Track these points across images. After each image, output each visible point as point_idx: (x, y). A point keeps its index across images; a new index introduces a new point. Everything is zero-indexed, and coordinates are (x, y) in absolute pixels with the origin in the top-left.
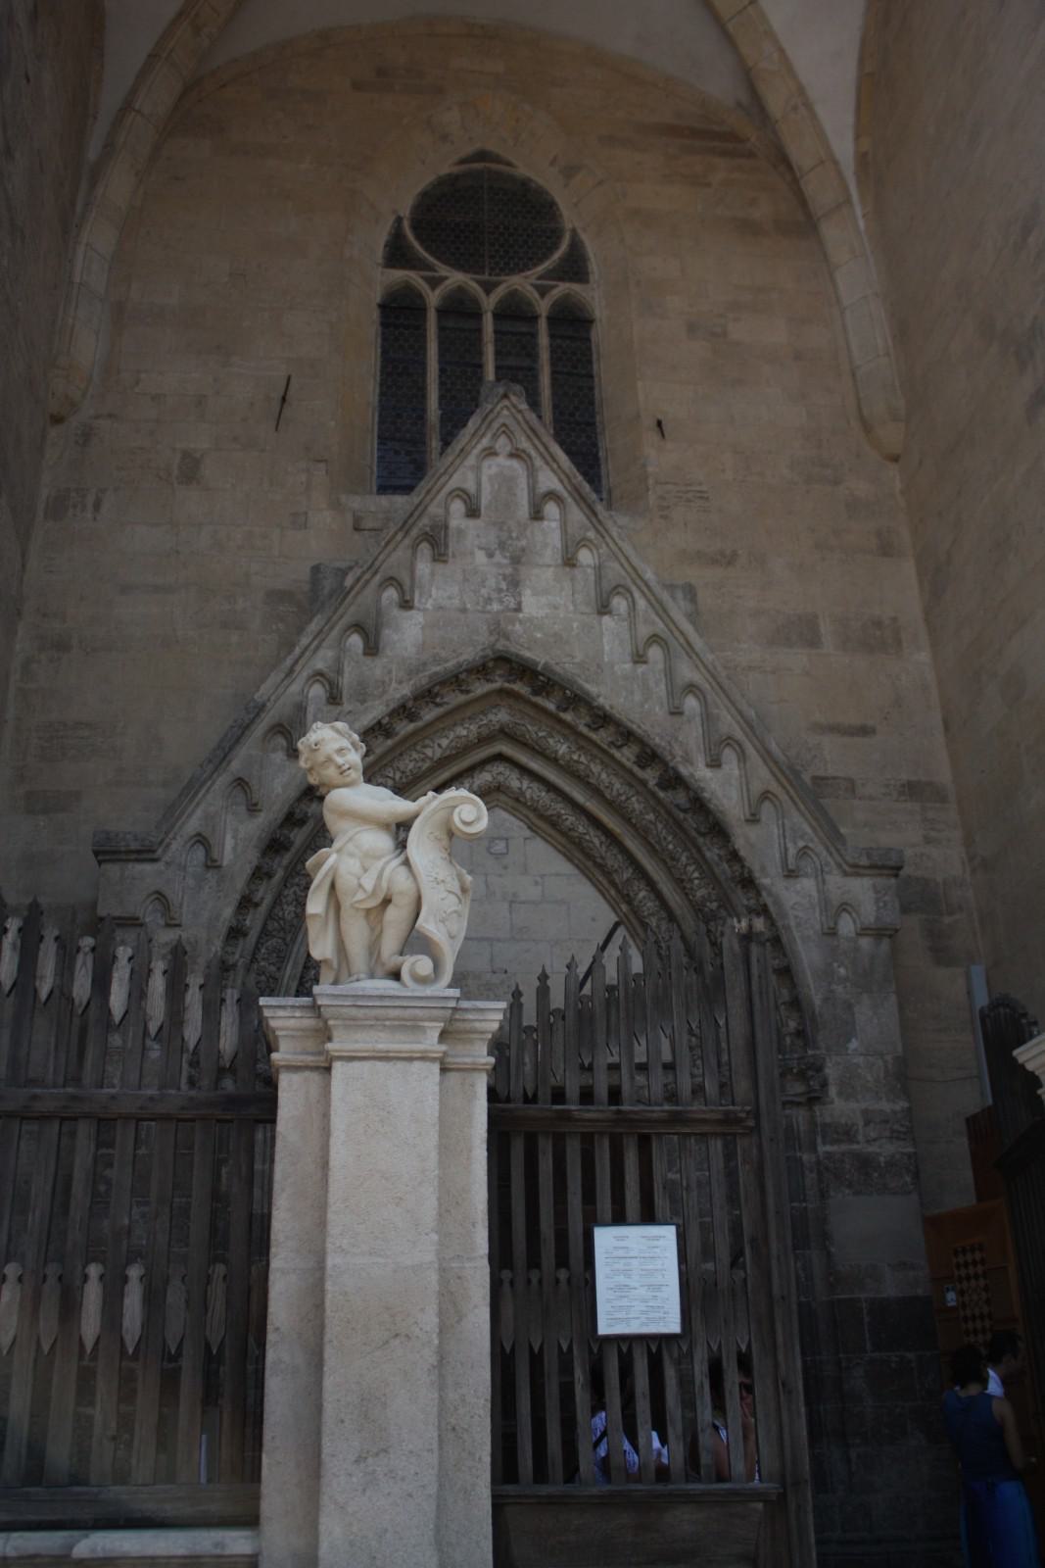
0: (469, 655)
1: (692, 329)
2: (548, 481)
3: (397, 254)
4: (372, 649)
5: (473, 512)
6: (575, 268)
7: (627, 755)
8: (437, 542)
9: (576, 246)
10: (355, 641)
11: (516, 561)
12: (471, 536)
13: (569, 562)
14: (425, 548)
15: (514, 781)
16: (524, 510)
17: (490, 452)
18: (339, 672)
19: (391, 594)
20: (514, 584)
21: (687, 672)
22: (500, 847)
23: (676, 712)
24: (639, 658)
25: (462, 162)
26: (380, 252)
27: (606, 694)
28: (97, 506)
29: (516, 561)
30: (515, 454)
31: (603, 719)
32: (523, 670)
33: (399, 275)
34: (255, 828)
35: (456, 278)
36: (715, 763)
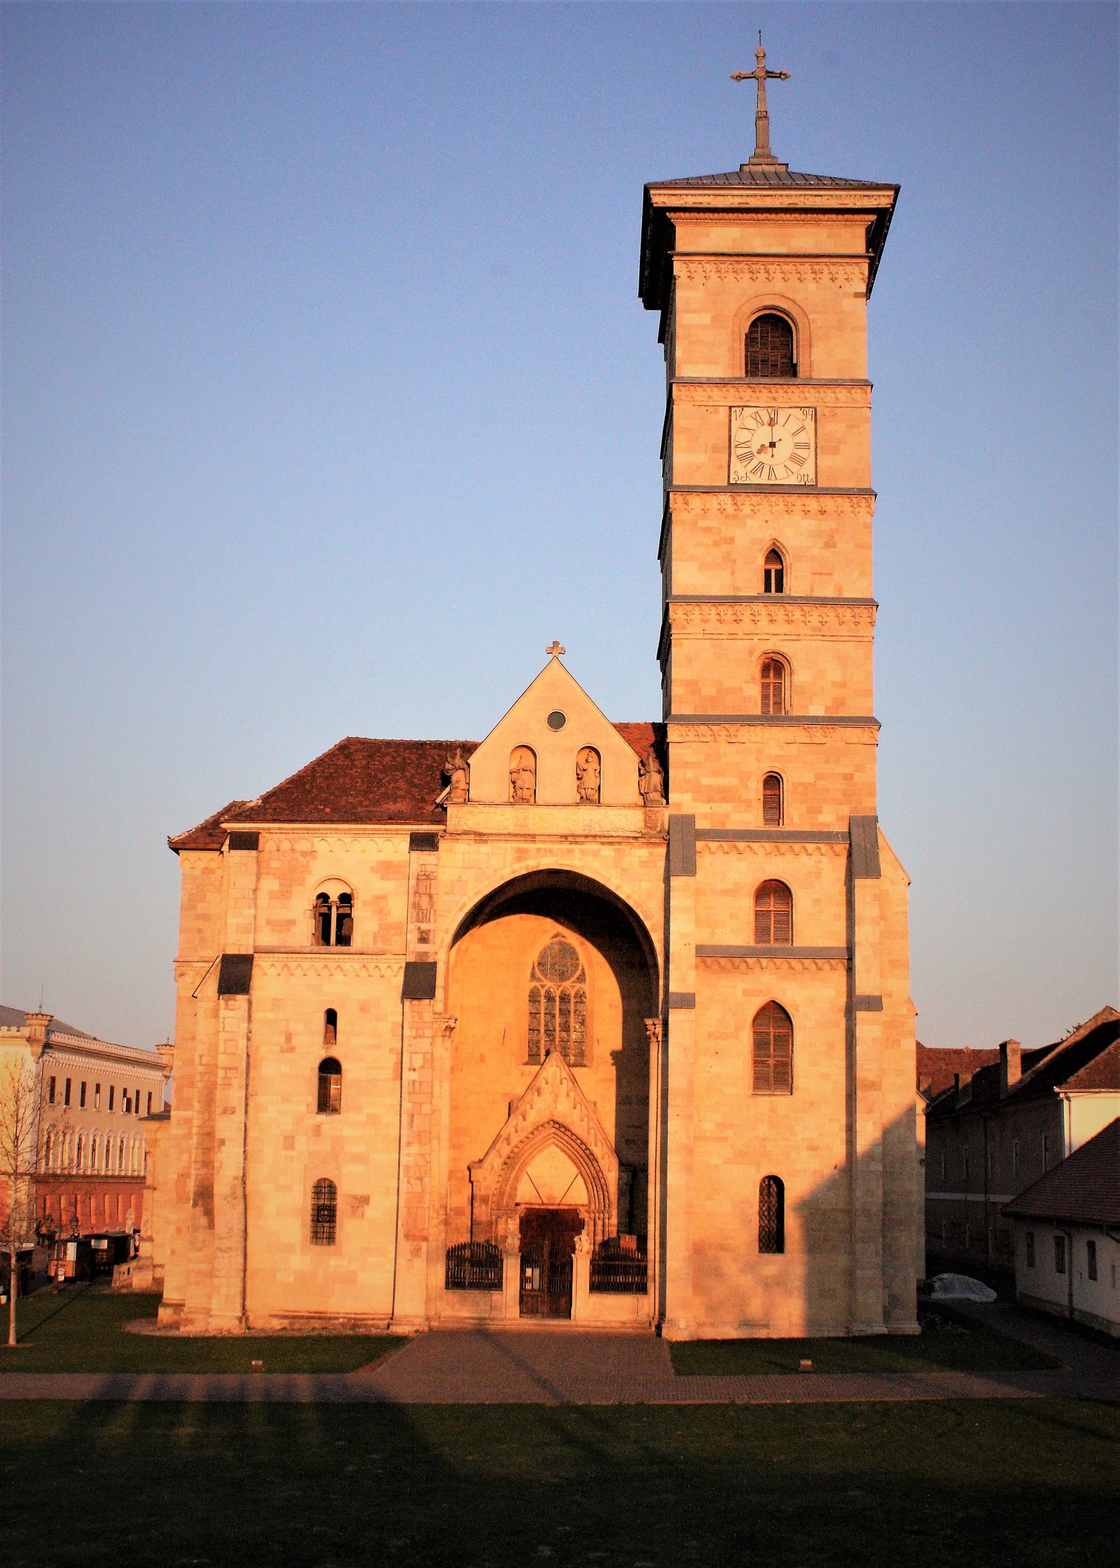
0: (545, 1120)
1: (610, 1006)
2: (564, 1075)
3: (533, 975)
4: (524, 1119)
5: (547, 1083)
6: (582, 979)
7: (579, 1142)
8: (539, 1092)
9: (583, 974)
10: (521, 1117)
11: (556, 1096)
12: (546, 1089)
13: (568, 1095)
14: (536, 1093)
15: (556, 1142)
16: (559, 1082)
17: (551, 1066)
18: (517, 1126)
19: (528, 1106)
20: (555, 1102)
21: (591, 1125)
22: (553, 1155)
23: (589, 1133)
24: (582, 1120)
25: (553, 938)
26: (528, 975)
27: (574, 1129)
28: (461, 1069)
29: (556, 1096)
30: (557, 1066)
31: (572, 1134)
32: (555, 1122)
33: (534, 984)
34: (501, 1161)
35: (549, 984)
36: (596, 1145)
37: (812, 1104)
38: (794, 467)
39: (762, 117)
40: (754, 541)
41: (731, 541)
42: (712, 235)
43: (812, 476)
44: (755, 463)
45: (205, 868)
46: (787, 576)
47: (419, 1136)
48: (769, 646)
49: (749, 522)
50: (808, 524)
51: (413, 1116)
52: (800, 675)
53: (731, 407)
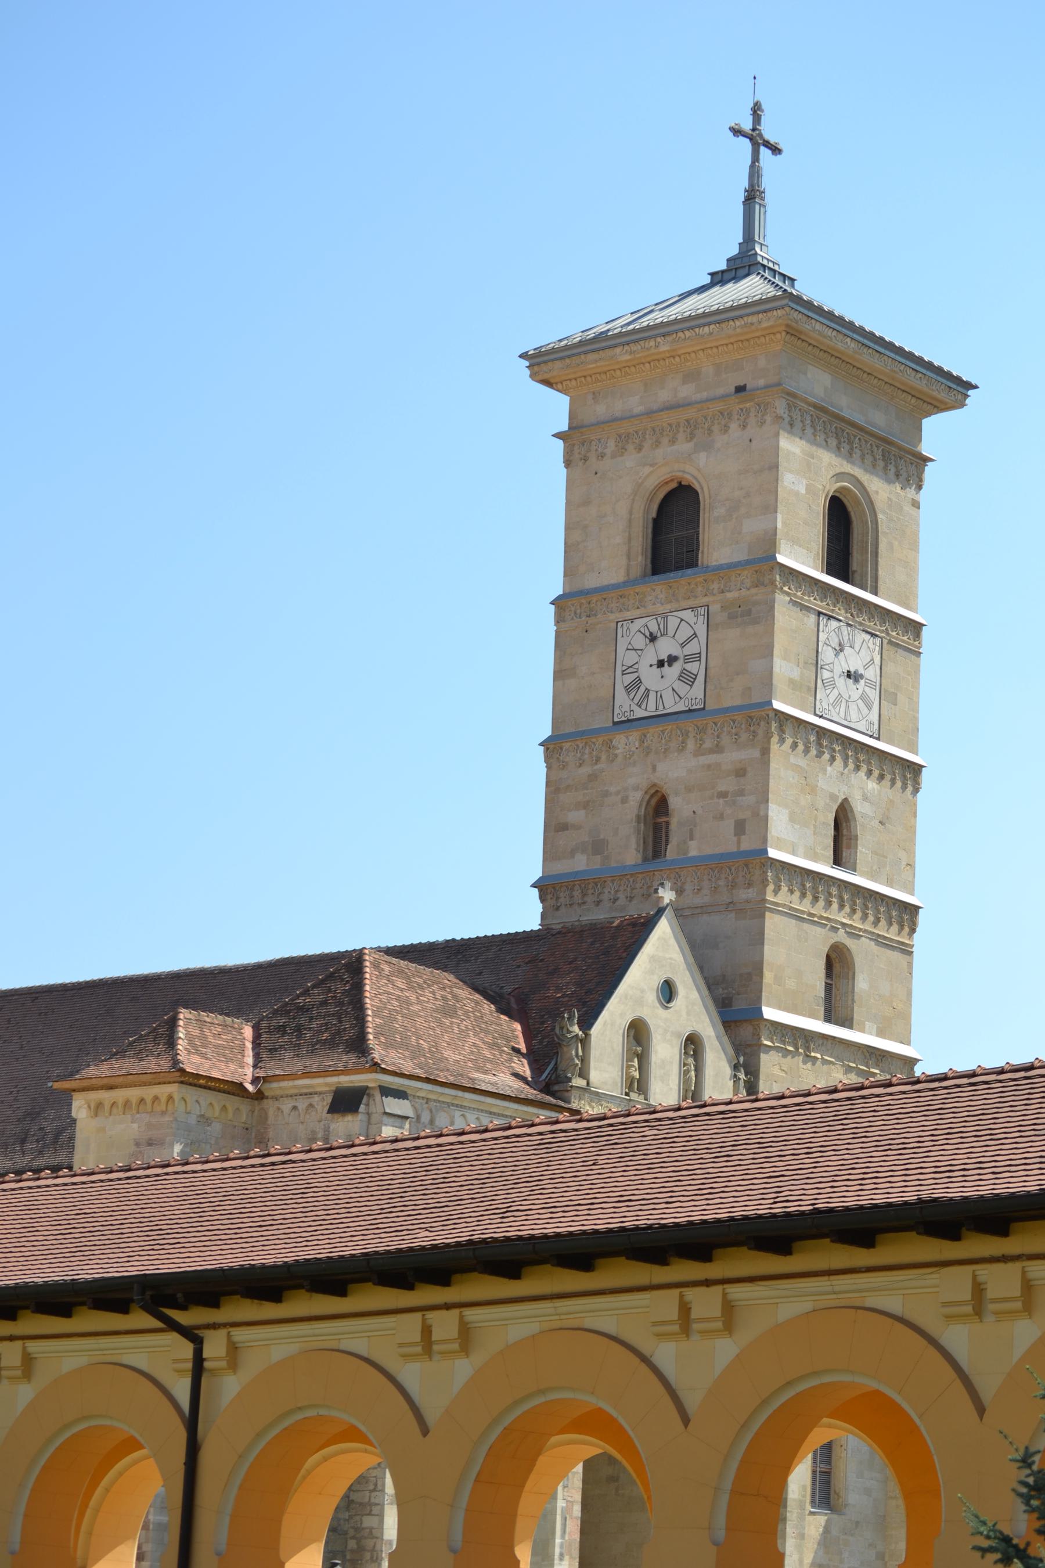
37: (857, 1523)
38: (865, 711)
39: (753, 196)
40: (833, 797)
41: (813, 790)
42: (809, 375)
43: (876, 726)
44: (835, 692)
45: (202, 1116)
46: (849, 847)
47: (570, 1545)
48: (841, 936)
49: (829, 768)
50: (872, 785)
51: (566, 1518)
52: (862, 983)
53: (820, 613)
